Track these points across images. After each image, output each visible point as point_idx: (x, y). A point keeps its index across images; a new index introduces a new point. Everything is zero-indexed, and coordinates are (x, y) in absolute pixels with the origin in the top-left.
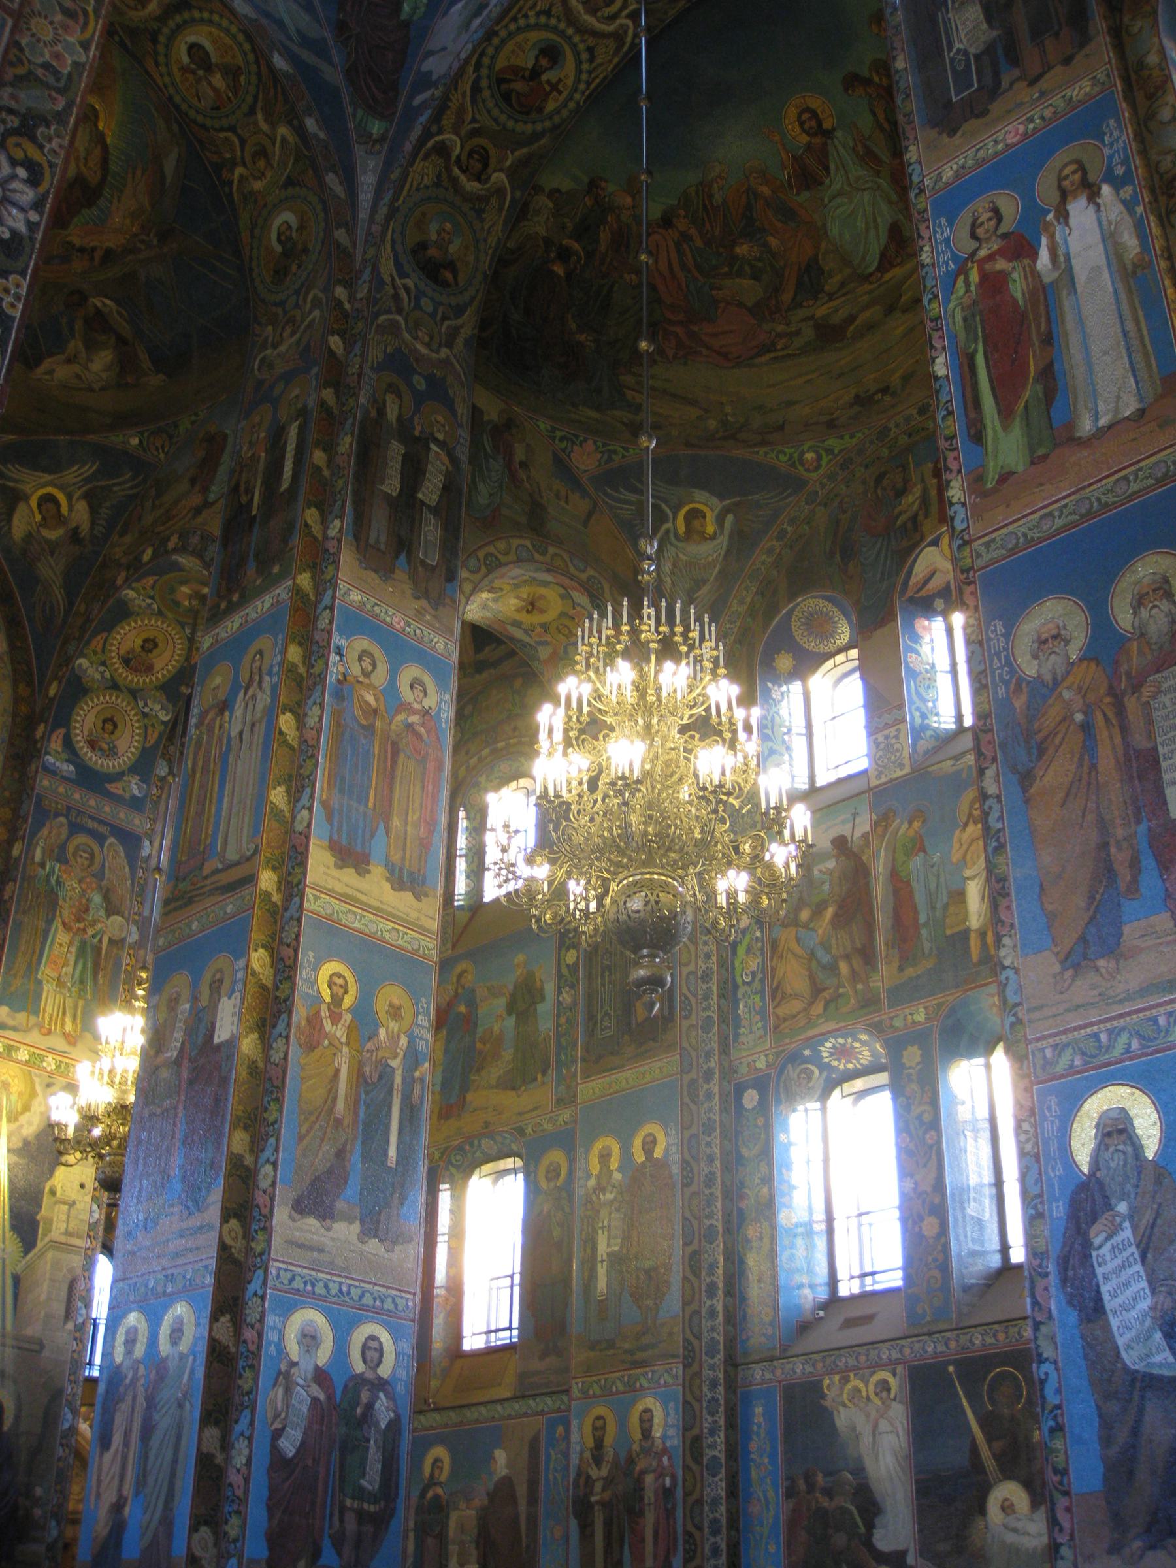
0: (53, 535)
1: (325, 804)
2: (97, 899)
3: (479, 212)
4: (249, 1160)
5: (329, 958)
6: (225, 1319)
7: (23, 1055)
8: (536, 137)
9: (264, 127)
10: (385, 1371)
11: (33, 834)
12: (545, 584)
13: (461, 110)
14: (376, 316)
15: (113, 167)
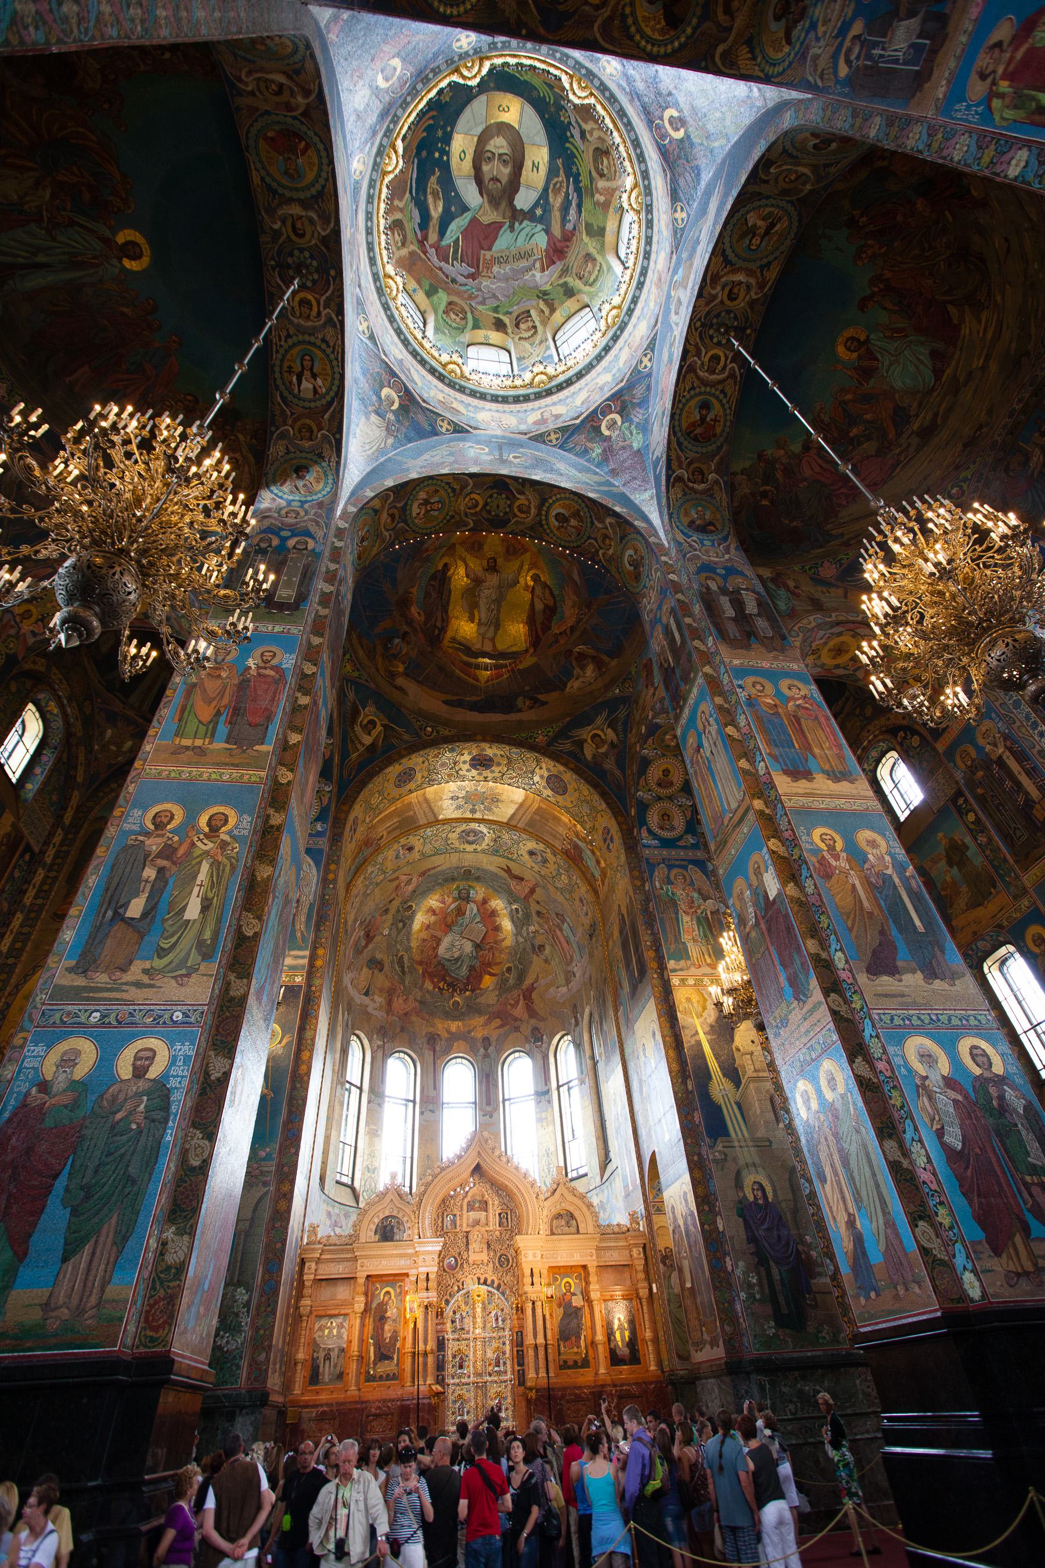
0: (603, 750)
1: (769, 754)
2: (696, 895)
3: (711, 496)
4: (824, 955)
5: (814, 827)
6: (859, 1059)
7: (691, 982)
8: (720, 448)
9: (600, 525)
10: (998, 1068)
11: (651, 876)
12: (840, 634)
13: (678, 458)
14: (684, 556)
15: (556, 593)
